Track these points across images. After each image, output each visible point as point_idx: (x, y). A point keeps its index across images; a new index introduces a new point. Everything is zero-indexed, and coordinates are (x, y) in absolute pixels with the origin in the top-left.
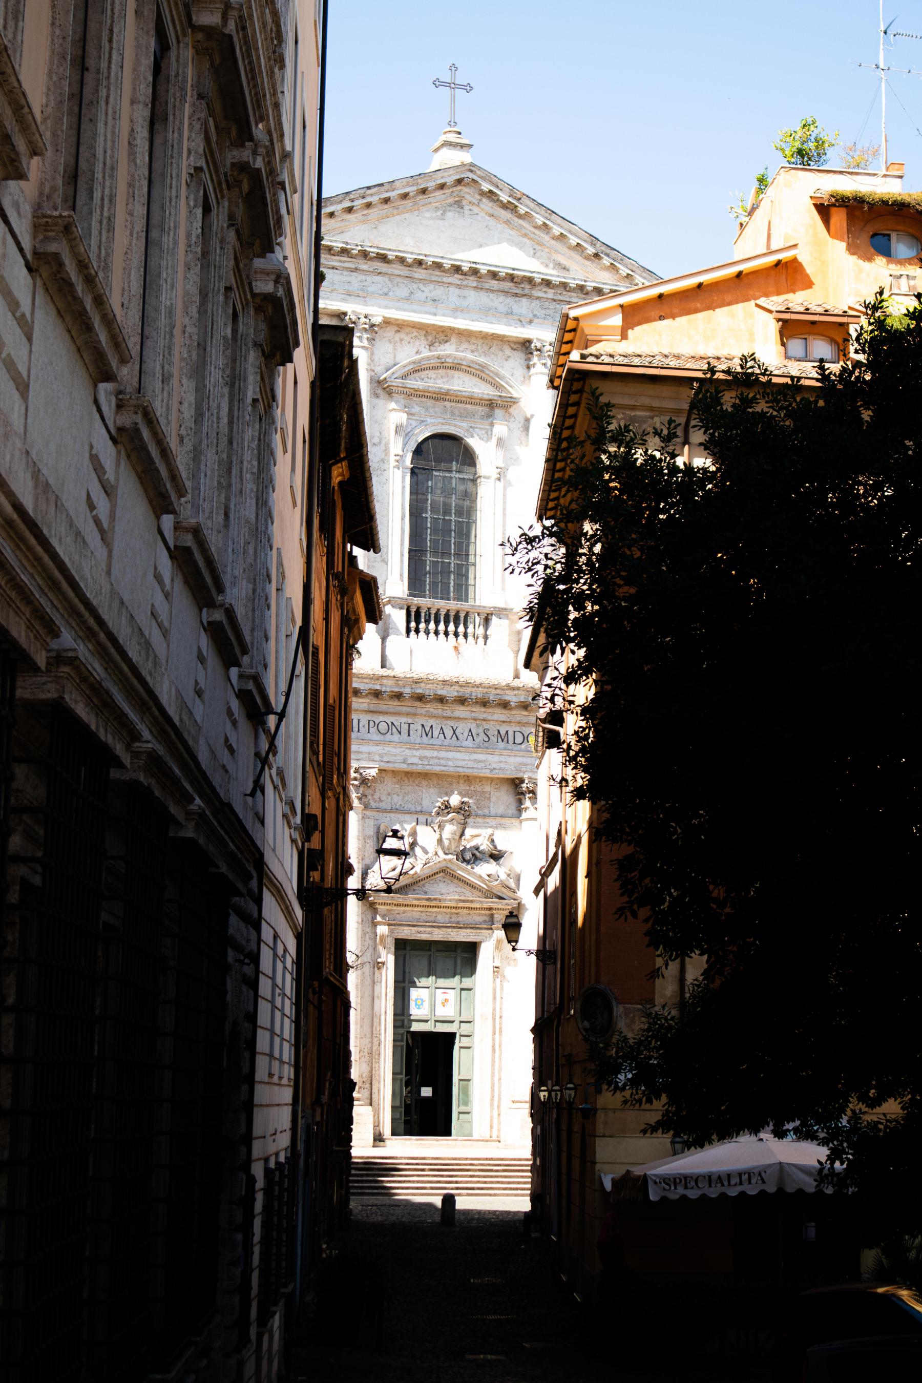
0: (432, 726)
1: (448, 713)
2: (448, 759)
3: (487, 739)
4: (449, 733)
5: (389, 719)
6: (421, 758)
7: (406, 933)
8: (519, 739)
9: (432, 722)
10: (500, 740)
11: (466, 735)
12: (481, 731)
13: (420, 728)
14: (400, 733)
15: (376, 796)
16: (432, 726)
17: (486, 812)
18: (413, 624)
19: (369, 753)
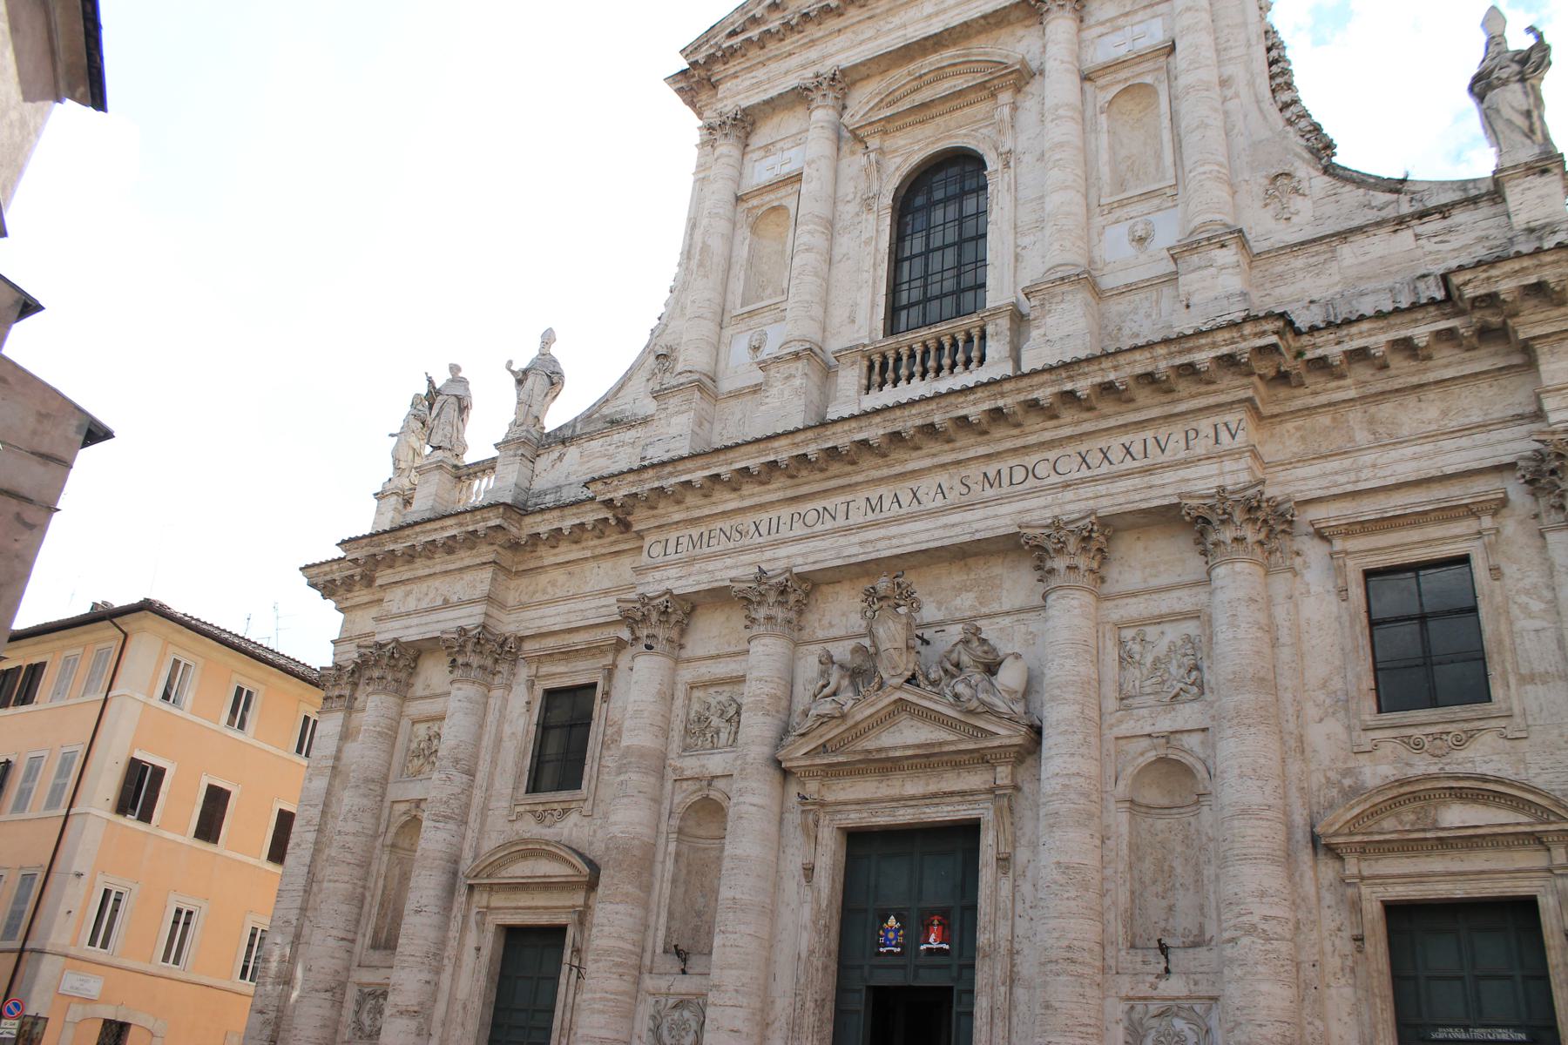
0: (881, 497)
1: (898, 469)
2: (903, 535)
3: (965, 490)
4: (905, 498)
5: (819, 504)
6: (861, 544)
7: (855, 819)
8: (1019, 475)
9: (884, 490)
10: (987, 485)
11: (932, 494)
12: (956, 482)
13: (863, 503)
14: (834, 518)
15: (825, 622)
16: (881, 497)
17: (995, 607)
18: (876, 378)
19: (788, 557)
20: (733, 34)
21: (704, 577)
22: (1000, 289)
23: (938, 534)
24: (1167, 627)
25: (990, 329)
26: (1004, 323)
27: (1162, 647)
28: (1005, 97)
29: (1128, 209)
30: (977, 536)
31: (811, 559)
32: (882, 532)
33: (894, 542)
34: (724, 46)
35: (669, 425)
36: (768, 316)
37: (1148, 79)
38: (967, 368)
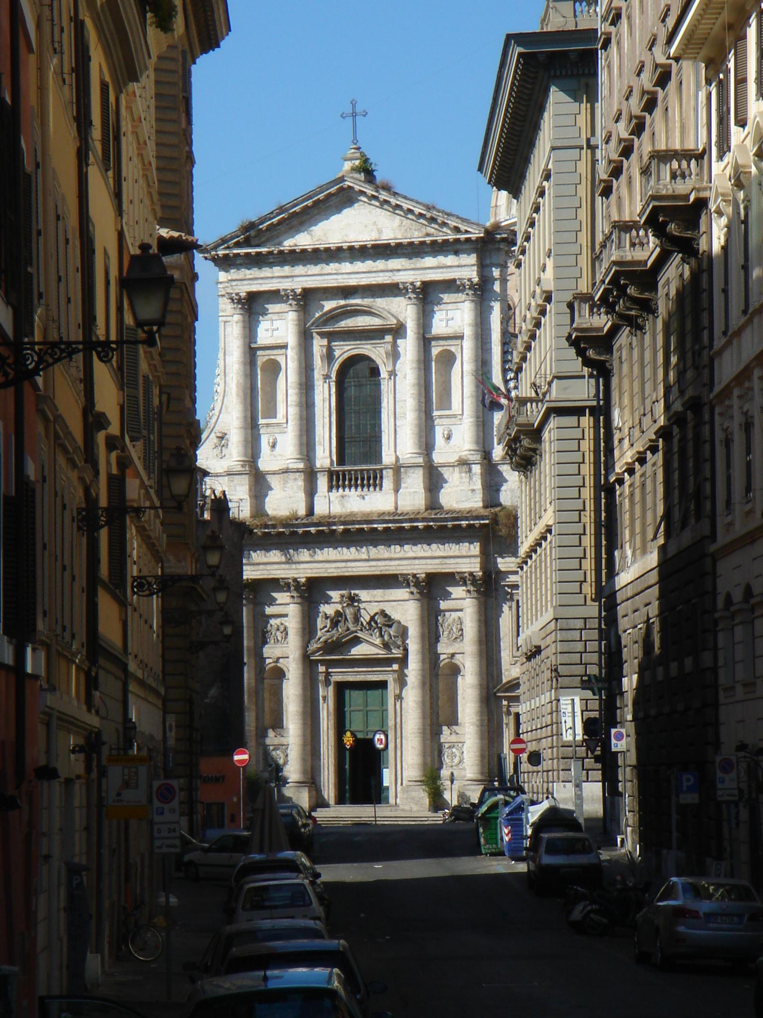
20: (238, 245)
21: (265, 572)
22: (388, 457)
23: (366, 569)
24: (452, 613)
25: (384, 472)
26: (390, 472)
27: (450, 620)
28: (389, 338)
29: (442, 420)
30: (382, 573)
31: (315, 571)
32: (343, 564)
33: (349, 569)
34: (235, 251)
35: (236, 490)
36: (276, 430)
37: (453, 349)
38: (375, 490)
